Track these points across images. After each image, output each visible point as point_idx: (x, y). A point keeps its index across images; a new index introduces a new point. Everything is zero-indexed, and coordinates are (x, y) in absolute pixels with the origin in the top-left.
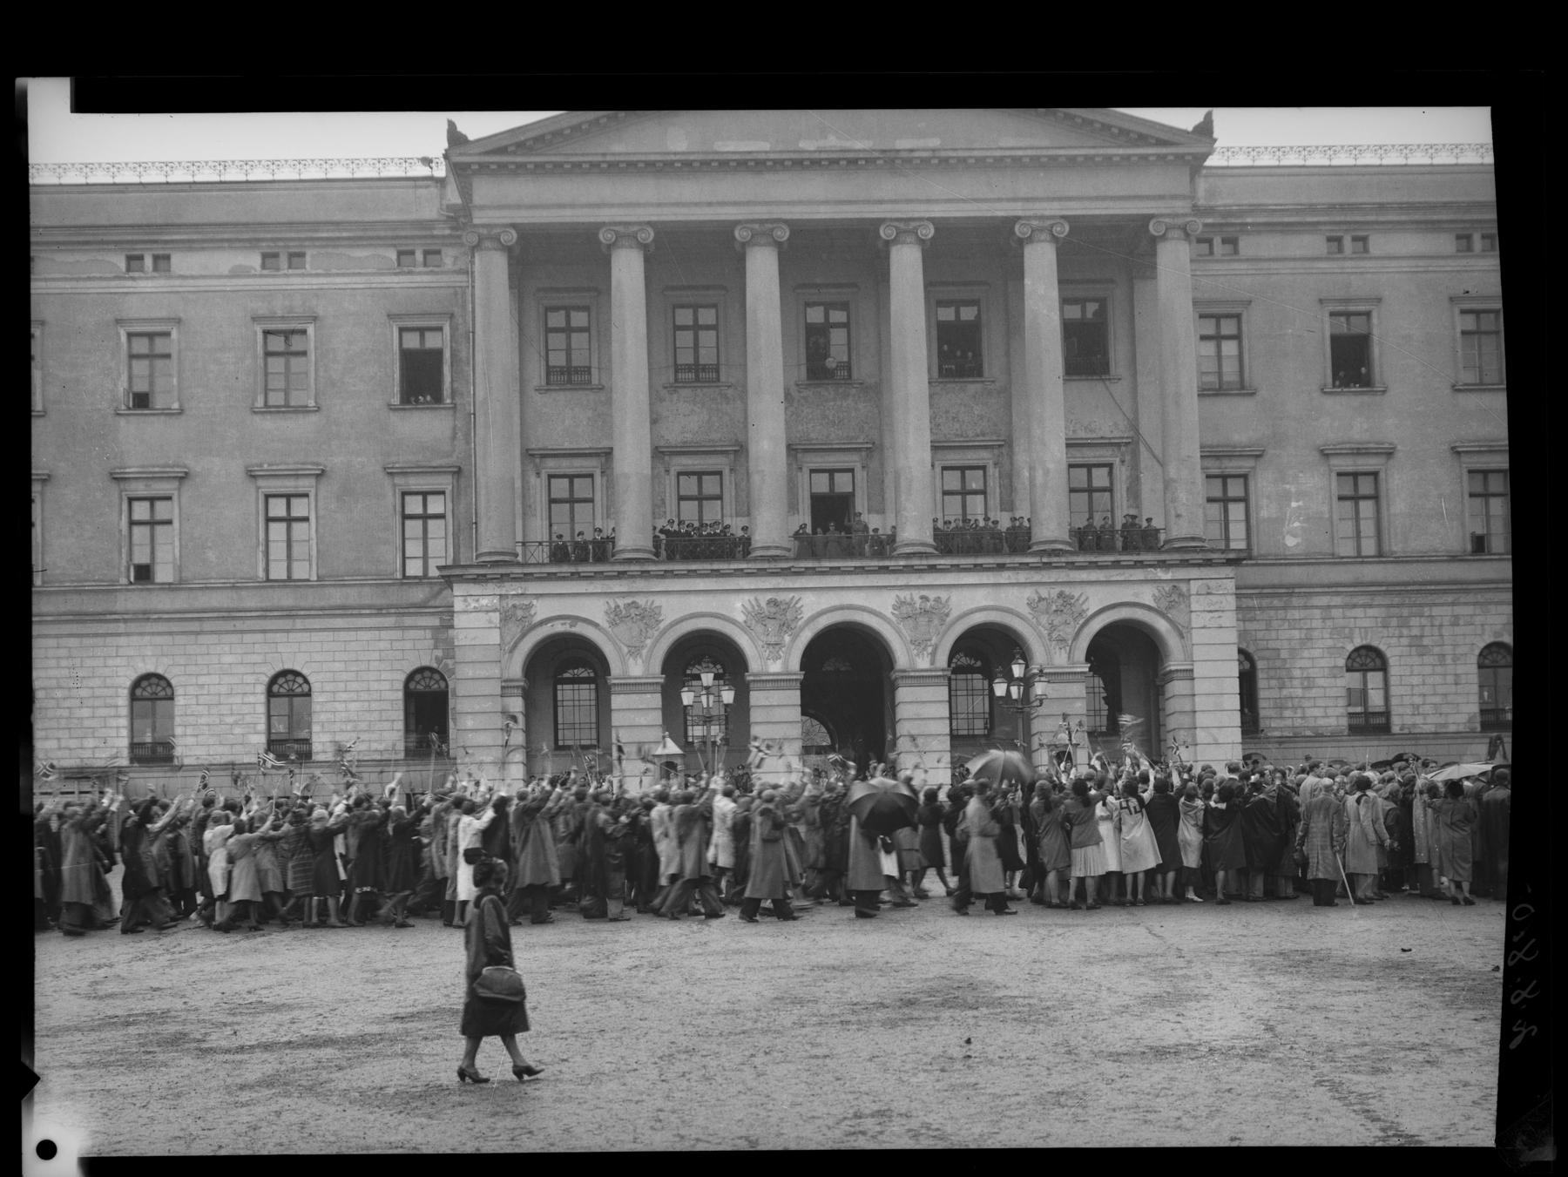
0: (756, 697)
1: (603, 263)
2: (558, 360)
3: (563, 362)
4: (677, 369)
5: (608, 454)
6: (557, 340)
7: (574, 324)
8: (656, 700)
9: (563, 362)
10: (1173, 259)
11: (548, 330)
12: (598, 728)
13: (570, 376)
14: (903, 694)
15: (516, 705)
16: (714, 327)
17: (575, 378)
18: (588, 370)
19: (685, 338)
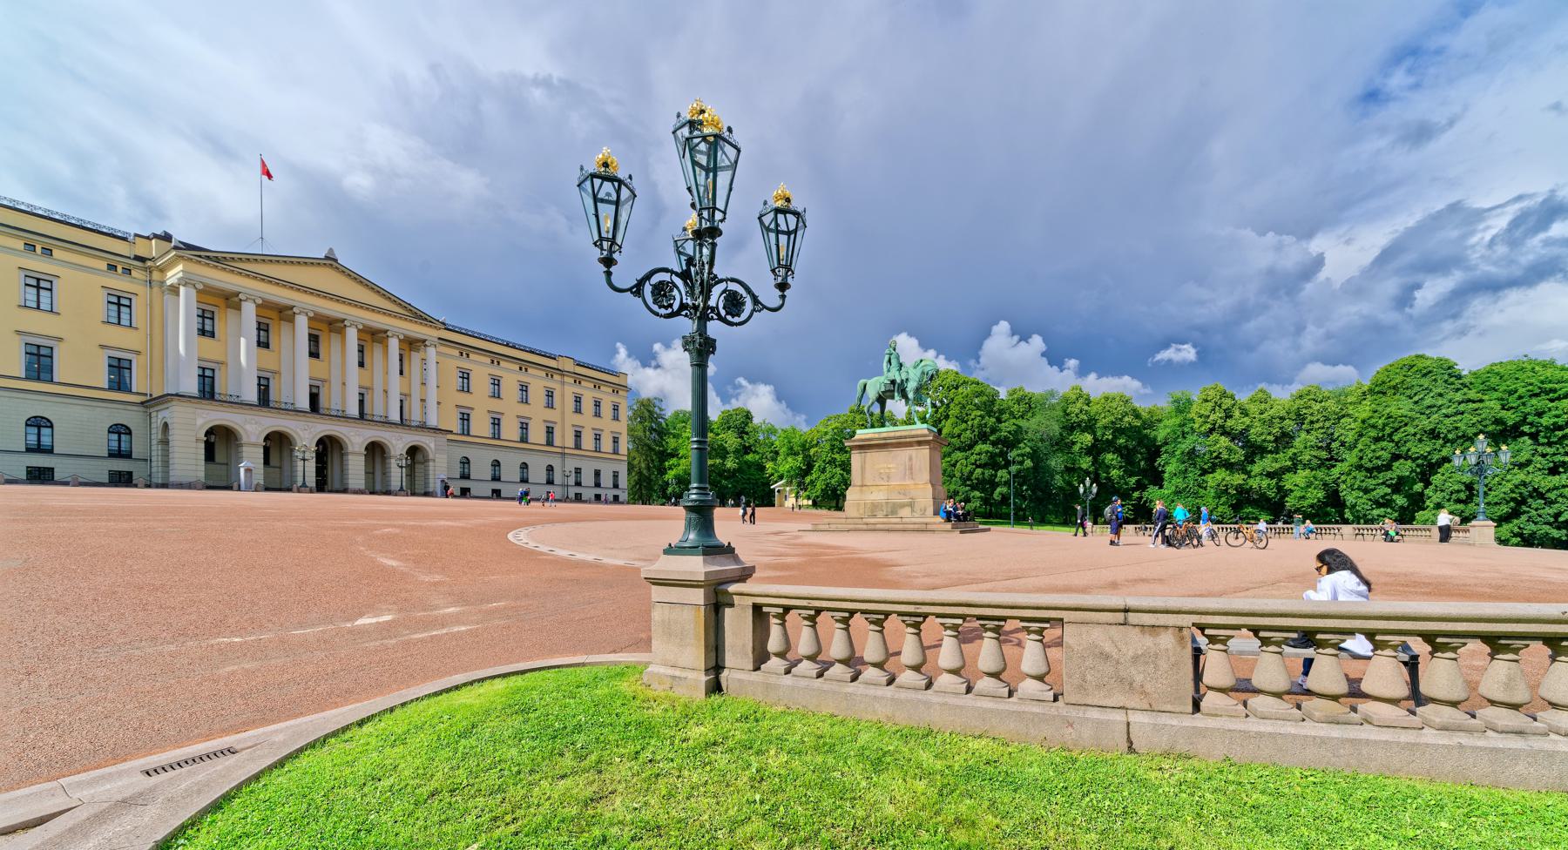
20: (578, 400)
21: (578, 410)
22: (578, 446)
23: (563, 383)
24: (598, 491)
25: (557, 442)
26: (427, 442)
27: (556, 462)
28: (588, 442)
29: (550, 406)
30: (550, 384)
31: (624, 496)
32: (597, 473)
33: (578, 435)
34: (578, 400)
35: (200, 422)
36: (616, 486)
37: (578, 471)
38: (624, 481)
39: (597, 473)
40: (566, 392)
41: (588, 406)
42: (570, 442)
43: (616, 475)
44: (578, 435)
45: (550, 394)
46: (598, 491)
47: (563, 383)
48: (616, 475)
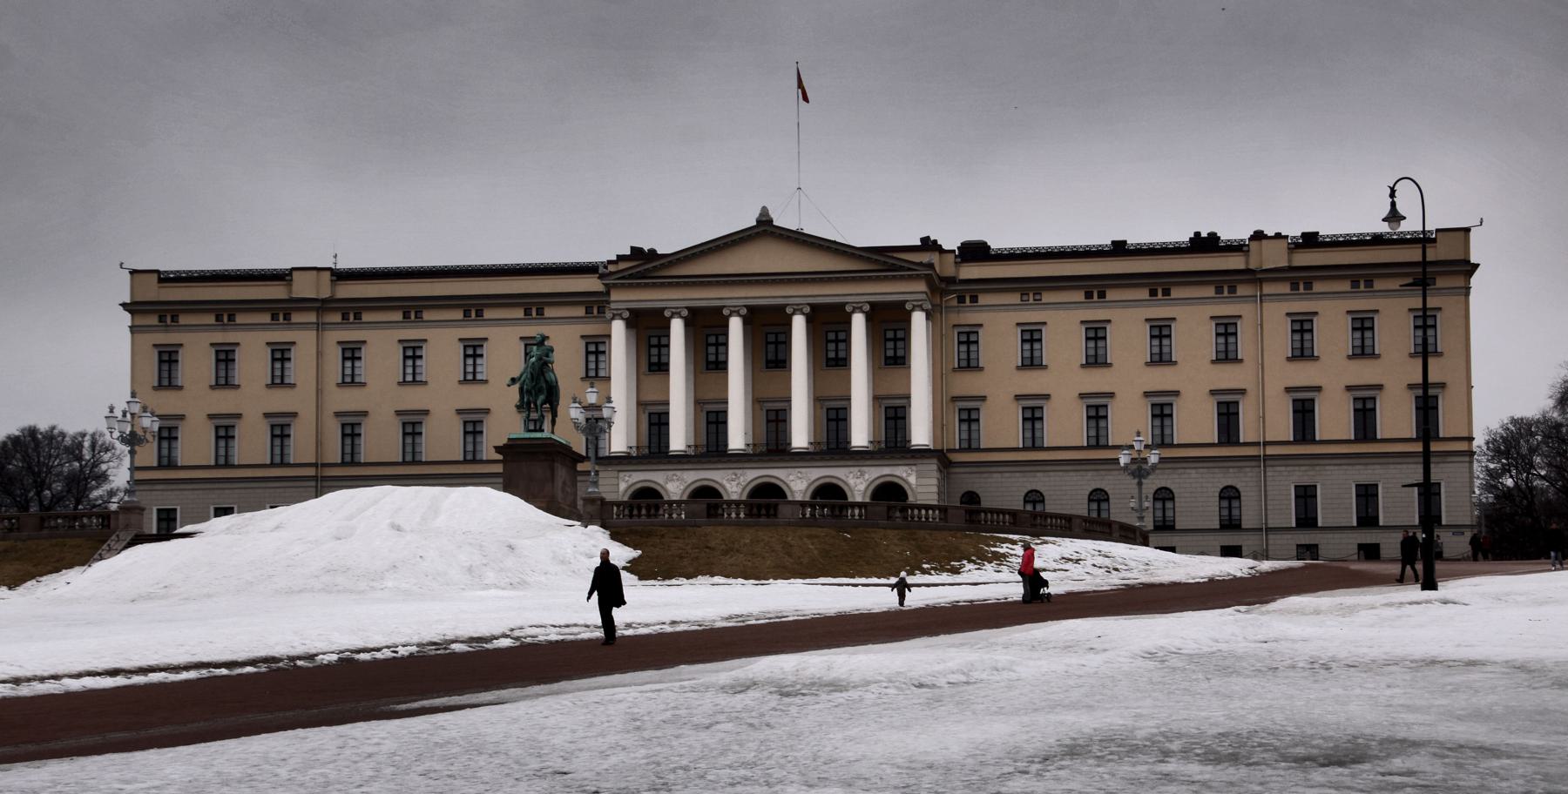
10: (918, 320)
11: (651, 346)
19: (712, 350)
20: (1302, 326)
21: (1302, 353)
24: (1369, 537)
25: (1247, 429)
27: (1244, 481)
28: (1334, 420)
29: (1227, 356)
33: (1304, 412)
34: (1302, 326)
35: (623, 486)
37: (1306, 496)
39: (1367, 494)
40: (1266, 323)
41: (1333, 331)
42: (1281, 425)
44: (1304, 412)
45: (1226, 329)
46: (1369, 537)
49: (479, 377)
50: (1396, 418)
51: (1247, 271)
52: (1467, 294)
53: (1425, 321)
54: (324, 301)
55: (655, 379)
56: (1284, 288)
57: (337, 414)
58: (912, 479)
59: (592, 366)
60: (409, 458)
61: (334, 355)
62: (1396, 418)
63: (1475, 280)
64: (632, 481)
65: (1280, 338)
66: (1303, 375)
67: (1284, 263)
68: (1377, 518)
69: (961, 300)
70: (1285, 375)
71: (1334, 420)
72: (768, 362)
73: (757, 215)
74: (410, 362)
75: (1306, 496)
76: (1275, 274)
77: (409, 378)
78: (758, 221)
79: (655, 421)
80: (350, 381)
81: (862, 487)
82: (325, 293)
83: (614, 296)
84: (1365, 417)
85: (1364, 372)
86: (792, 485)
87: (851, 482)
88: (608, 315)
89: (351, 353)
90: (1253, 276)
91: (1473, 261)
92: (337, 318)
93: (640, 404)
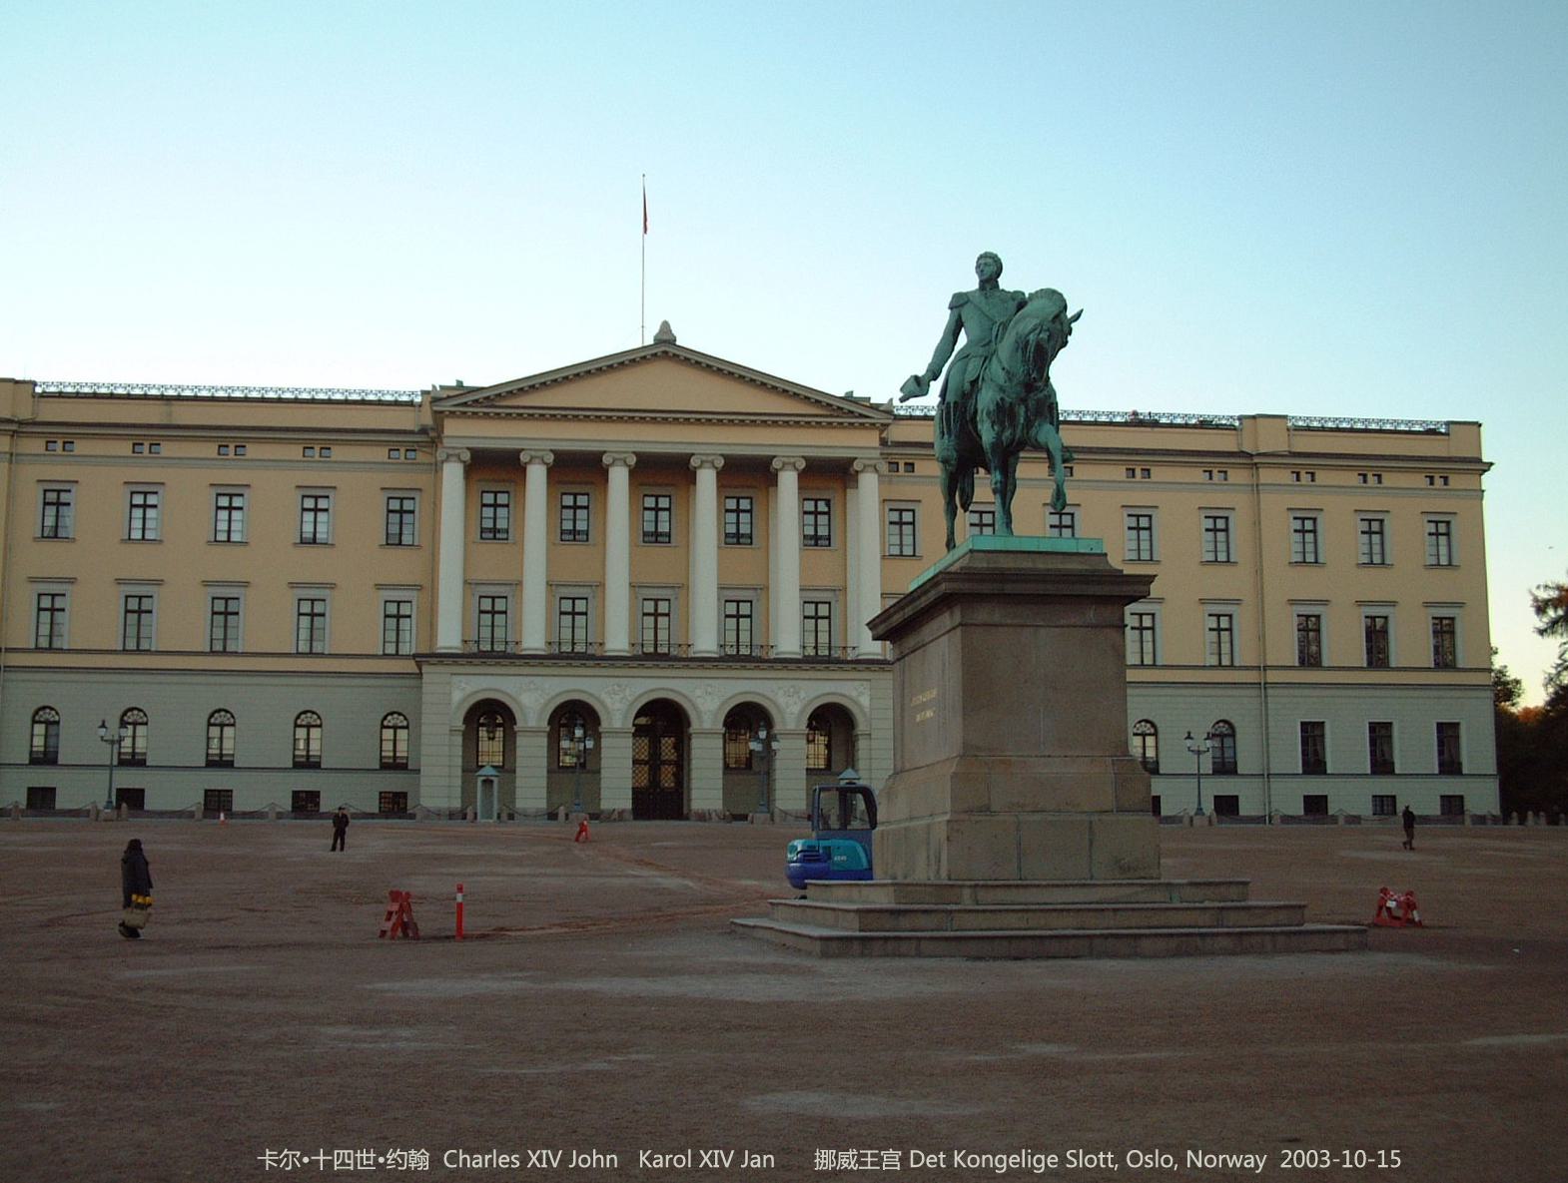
0: (605, 742)
1: (524, 470)
2: (489, 524)
3: (491, 525)
4: (563, 532)
5: (520, 584)
6: (488, 512)
7: (499, 502)
8: (544, 741)
9: (491, 525)
10: (869, 485)
12: (504, 756)
13: (493, 533)
14: (695, 743)
15: (459, 740)
16: (587, 508)
17: (498, 536)
18: (507, 531)
20: (1307, 525)
21: (1309, 560)
22: (1310, 659)
23: (1256, 488)
26: (860, 695)
27: (1241, 710)
28: (1344, 643)
30: (1219, 499)
31: (1483, 796)
32: (1380, 734)
33: (1310, 629)
34: (1307, 525)
35: (457, 696)
36: (1450, 766)
37: (1312, 734)
38: (1479, 750)
39: (1380, 734)
41: (1341, 535)
42: (1284, 647)
43: (1448, 733)
44: (1310, 629)
45: (1219, 525)
47: (1256, 488)
48: (1448, 733)
49: (235, 537)
50: (1411, 644)
51: (1242, 454)
52: (1482, 499)
53: (1441, 528)
54: (20, 423)
55: (493, 548)
56: (1285, 476)
57: (33, 580)
58: (865, 701)
59: (394, 529)
60: (131, 645)
61: (32, 497)
62: (1411, 644)
63: (1487, 480)
64: (469, 689)
65: (1281, 540)
66: (1309, 584)
67: (1283, 448)
68: (1460, 764)
69: (894, 466)
70: (1286, 584)
71: (1344, 643)
72: (645, 534)
73: (656, 330)
74: (138, 513)
75: (1312, 734)
76: (1273, 459)
77: (137, 535)
78: (658, 341)
79: (492, 603)
80: (55, 534)
81: (796, 709)
82: (25, 414)
83: (451, 428)
84: (1376, 637)
85: (1375, 586)
86: (699, 702)
87: (781, 700)
88: (441, 454)
89: (56, 499)
90: (1248, 460)
91: (1485, 460)
92: (36, 446)
93: (466, 582)
